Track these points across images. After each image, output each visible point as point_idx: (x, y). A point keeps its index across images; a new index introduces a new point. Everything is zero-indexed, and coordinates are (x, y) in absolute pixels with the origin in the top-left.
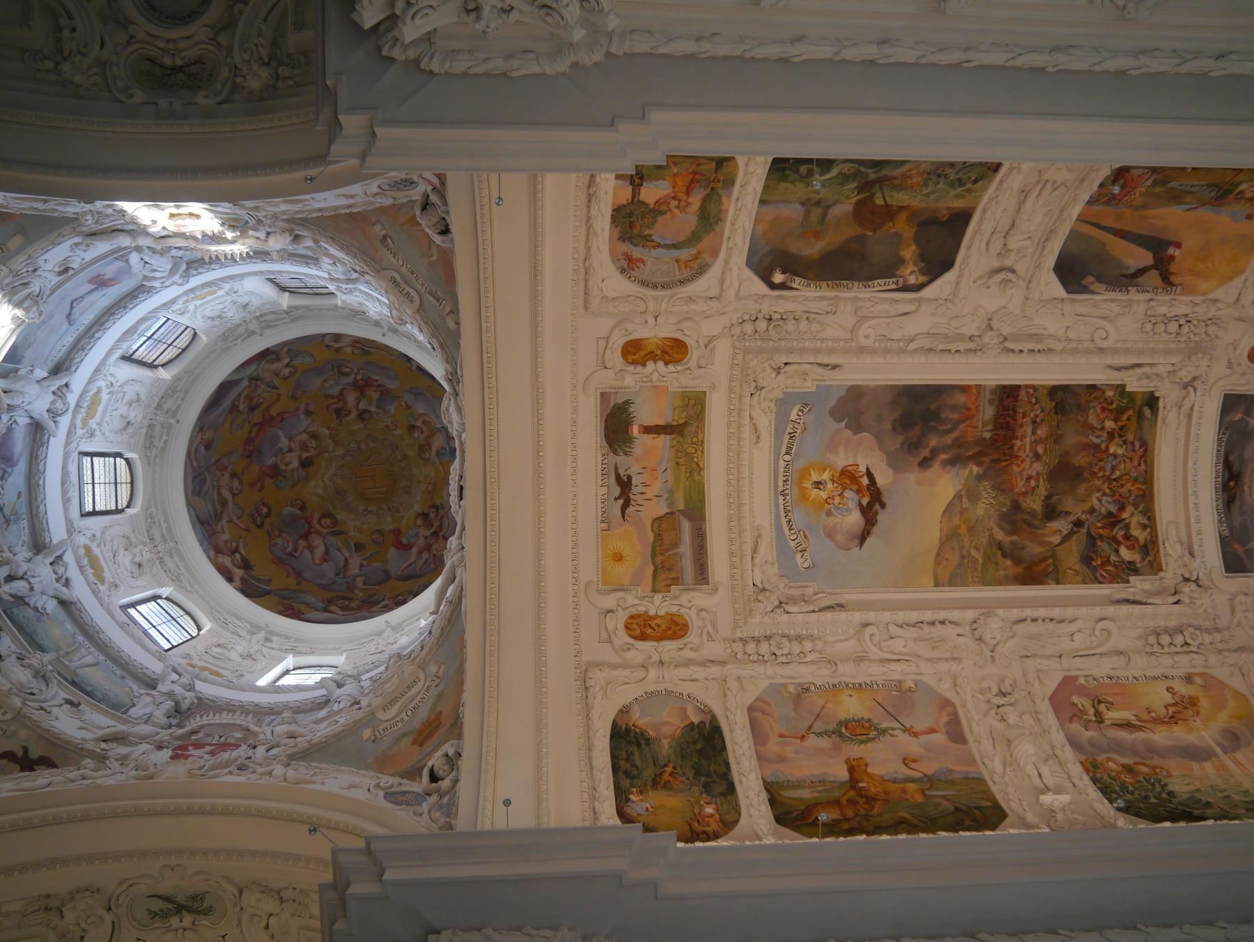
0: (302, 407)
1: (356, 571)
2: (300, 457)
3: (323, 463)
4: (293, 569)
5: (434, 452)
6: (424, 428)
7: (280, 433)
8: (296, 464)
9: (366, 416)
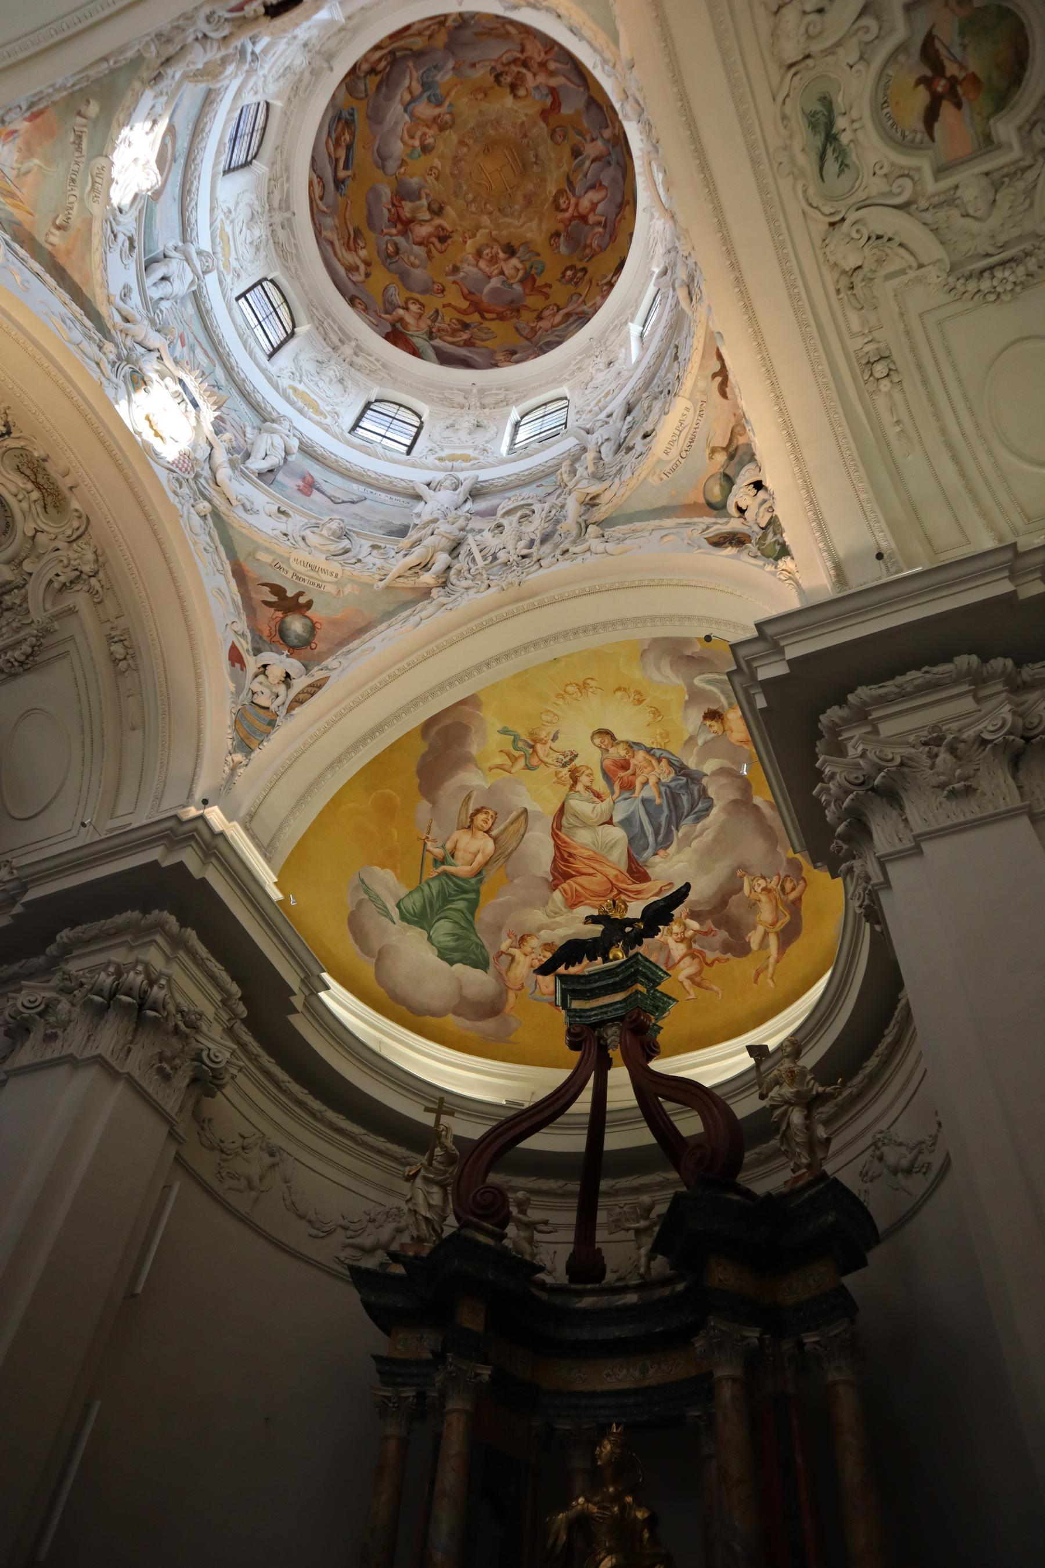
0: (451, 278)
1: (599, 143)
2: (506, 260)
3: (504, 233)
4: (617, 215)
5: (437, 111)
6: (418, 134)
7: (487, 289)
8: (514, 262)
9: (435, 207)
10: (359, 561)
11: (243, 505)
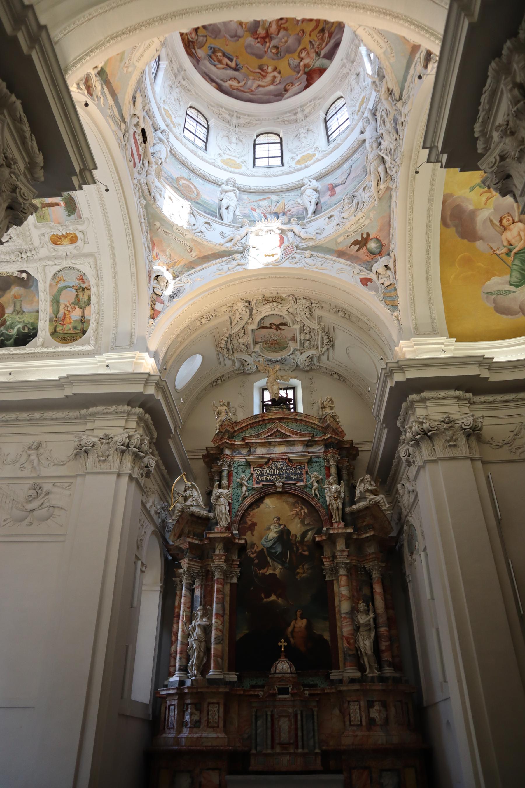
10: (364, 202)
11: (317, 233)
